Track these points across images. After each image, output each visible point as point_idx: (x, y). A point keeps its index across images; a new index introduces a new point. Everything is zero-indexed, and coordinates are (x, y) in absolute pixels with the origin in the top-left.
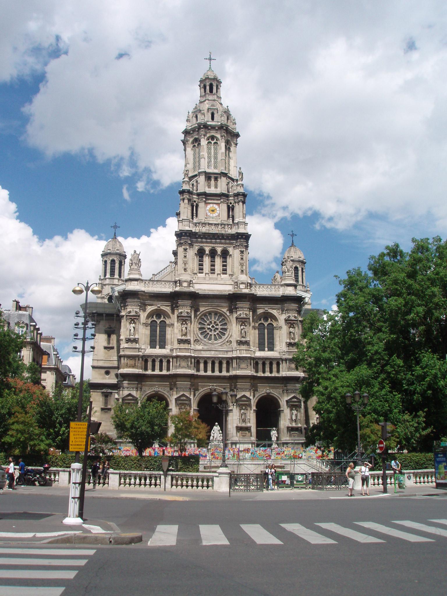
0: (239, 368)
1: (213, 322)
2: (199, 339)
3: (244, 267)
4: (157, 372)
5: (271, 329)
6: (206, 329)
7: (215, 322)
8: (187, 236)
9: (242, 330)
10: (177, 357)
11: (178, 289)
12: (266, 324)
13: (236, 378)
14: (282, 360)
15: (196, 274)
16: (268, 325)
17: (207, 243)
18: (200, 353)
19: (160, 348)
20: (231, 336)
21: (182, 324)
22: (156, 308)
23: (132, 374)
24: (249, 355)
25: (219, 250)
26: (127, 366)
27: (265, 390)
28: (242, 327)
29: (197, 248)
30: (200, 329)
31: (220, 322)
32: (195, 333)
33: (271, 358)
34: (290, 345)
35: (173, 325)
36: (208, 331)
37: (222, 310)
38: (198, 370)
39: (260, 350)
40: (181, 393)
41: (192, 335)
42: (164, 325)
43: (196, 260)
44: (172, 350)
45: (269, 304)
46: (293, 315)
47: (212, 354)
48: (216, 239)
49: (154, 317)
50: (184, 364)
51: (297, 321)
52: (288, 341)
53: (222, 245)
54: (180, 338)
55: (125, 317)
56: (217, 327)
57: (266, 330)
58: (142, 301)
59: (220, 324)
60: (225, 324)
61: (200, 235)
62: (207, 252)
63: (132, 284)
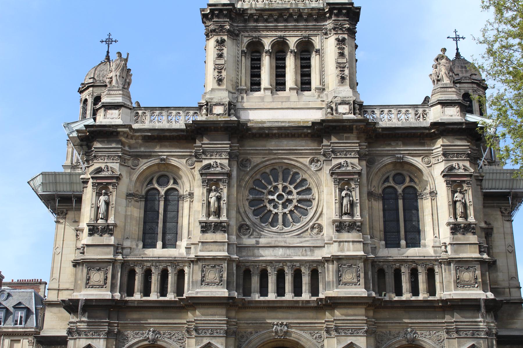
0: (339, 281)
1: (280, 187)
2: (248, 223)
3: (347, 72)
4: (154, 296)
5: (412, 198)
6: (266, 202)
7: (284, 188)
8: (225, 16)
9: (343, 197)
10: (198, 259)
11: (202, 117)
12: (400, 189)
13: (332, 304)
14: (440, 262)
15: (241, 91)
16: (404, 190)
17: (268, 29)
18: (250, 253)
19: (164, 246)
20: (321, 214)
21: (209, 191)
22: (157, 161)
23: (96, 300)
24: (362, 253)
25: (292, 42)
26: (88, 284)
27: (402, 334)
28: (344, 193)
29: (246, 40)
30: (252, 203)
31: (295, 188)
32: (242, 210)
33: (413, 261)
34: (455, 229)
35: (191, 195)
36: (270, 207)
37: (301, 160)
38: (247, 292)
39: (387, 246)
40: (206, 341)
41: (234, 213)
42: (173, 199)
43: (246, 63)
44: (188, 248)
45: (405, 144)
46: (461, 164)
47: (279, 254)
48: (286, 21)
49: (154, 182)
50: (212, 276)
51: (470, 176)
52: (452, 220)
53: (299, 33)
54: (204, 219)
55: (91, 181)
56: (290, 197)
57: (400, 202)
58: (127, 148)
59: (295, 192)
60: (309, 190)
61: (252, 15)
62: (267, 47)
63: (108, 115)
